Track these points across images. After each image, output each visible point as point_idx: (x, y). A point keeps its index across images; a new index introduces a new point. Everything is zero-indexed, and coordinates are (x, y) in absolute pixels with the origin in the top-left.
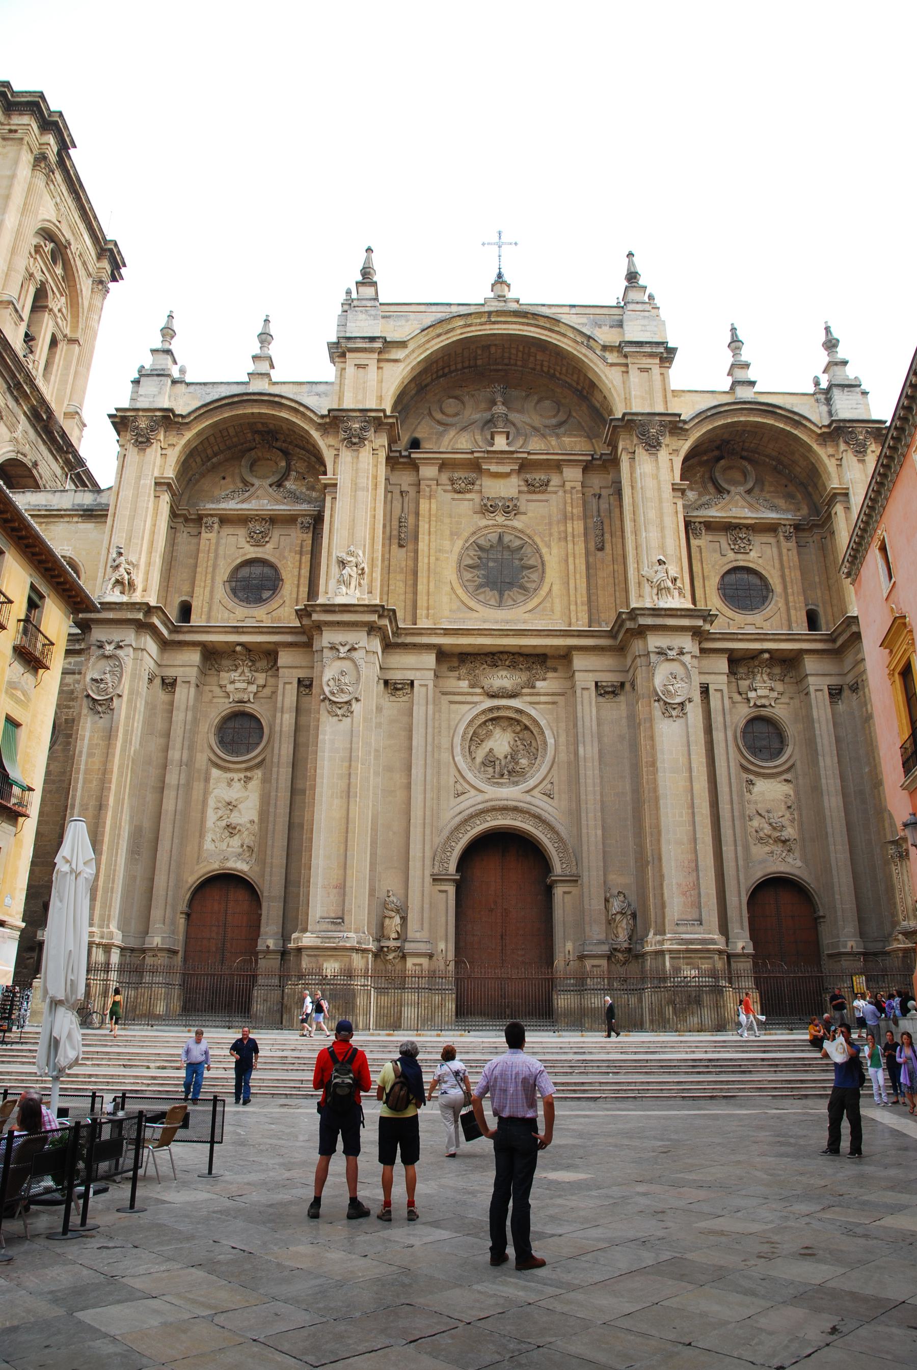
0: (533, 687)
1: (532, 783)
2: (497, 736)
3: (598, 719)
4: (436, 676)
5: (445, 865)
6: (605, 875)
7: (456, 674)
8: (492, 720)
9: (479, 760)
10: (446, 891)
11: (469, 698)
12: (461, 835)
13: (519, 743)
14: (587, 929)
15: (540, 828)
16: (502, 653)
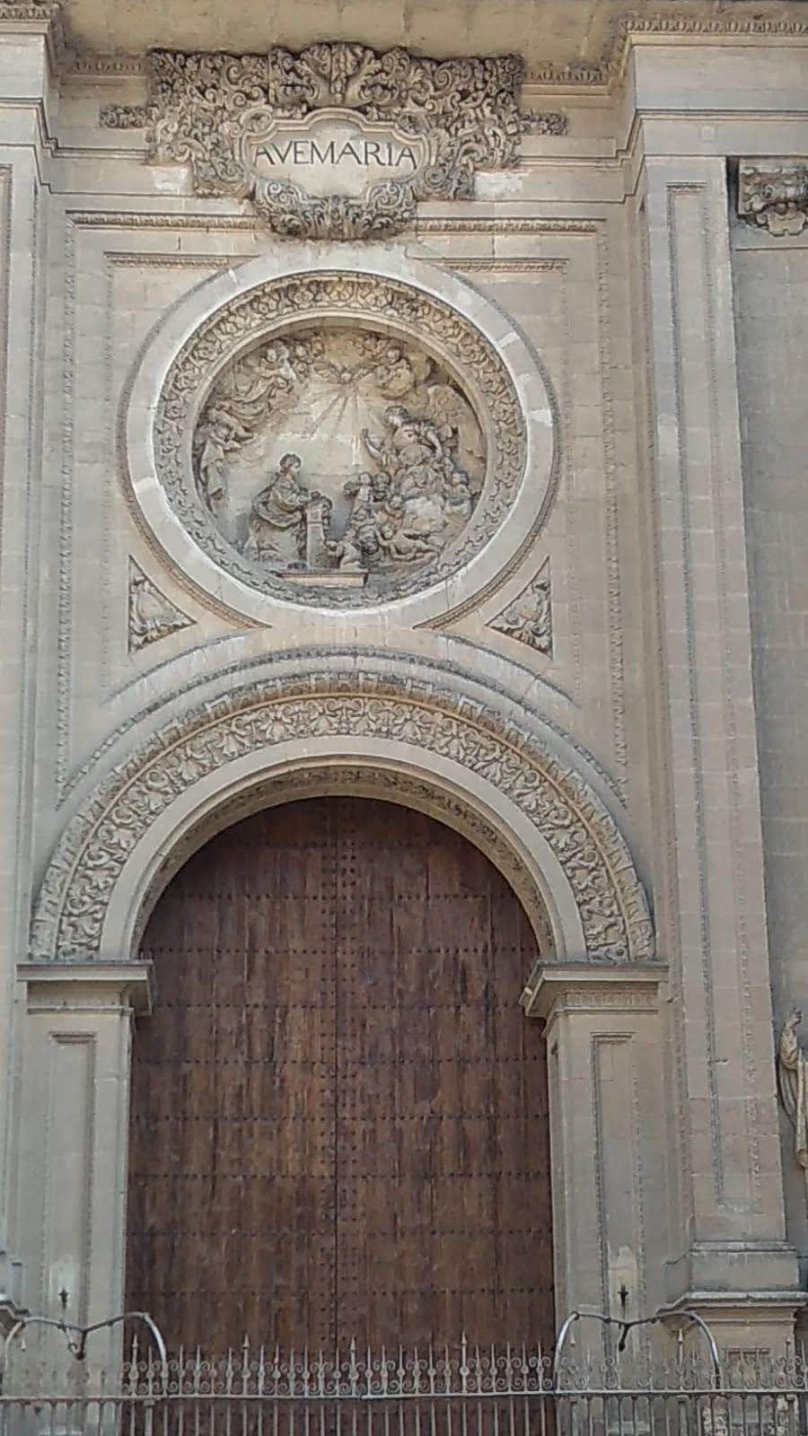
0: (466, 194)
1: (461, 585)
2: (316, 410)
3: (739, 317)
4: (53, 145)
5: (86, 925)
6: (774, 959)
7: (136, 137)
8: (291, 338)
9: (237, 504)
10: (87, 1039)
11: (193, 242)
12: (155, 801)
13: (405, 435)
14: (704, 1189)
15: (494, 768)
16: (329, 45)
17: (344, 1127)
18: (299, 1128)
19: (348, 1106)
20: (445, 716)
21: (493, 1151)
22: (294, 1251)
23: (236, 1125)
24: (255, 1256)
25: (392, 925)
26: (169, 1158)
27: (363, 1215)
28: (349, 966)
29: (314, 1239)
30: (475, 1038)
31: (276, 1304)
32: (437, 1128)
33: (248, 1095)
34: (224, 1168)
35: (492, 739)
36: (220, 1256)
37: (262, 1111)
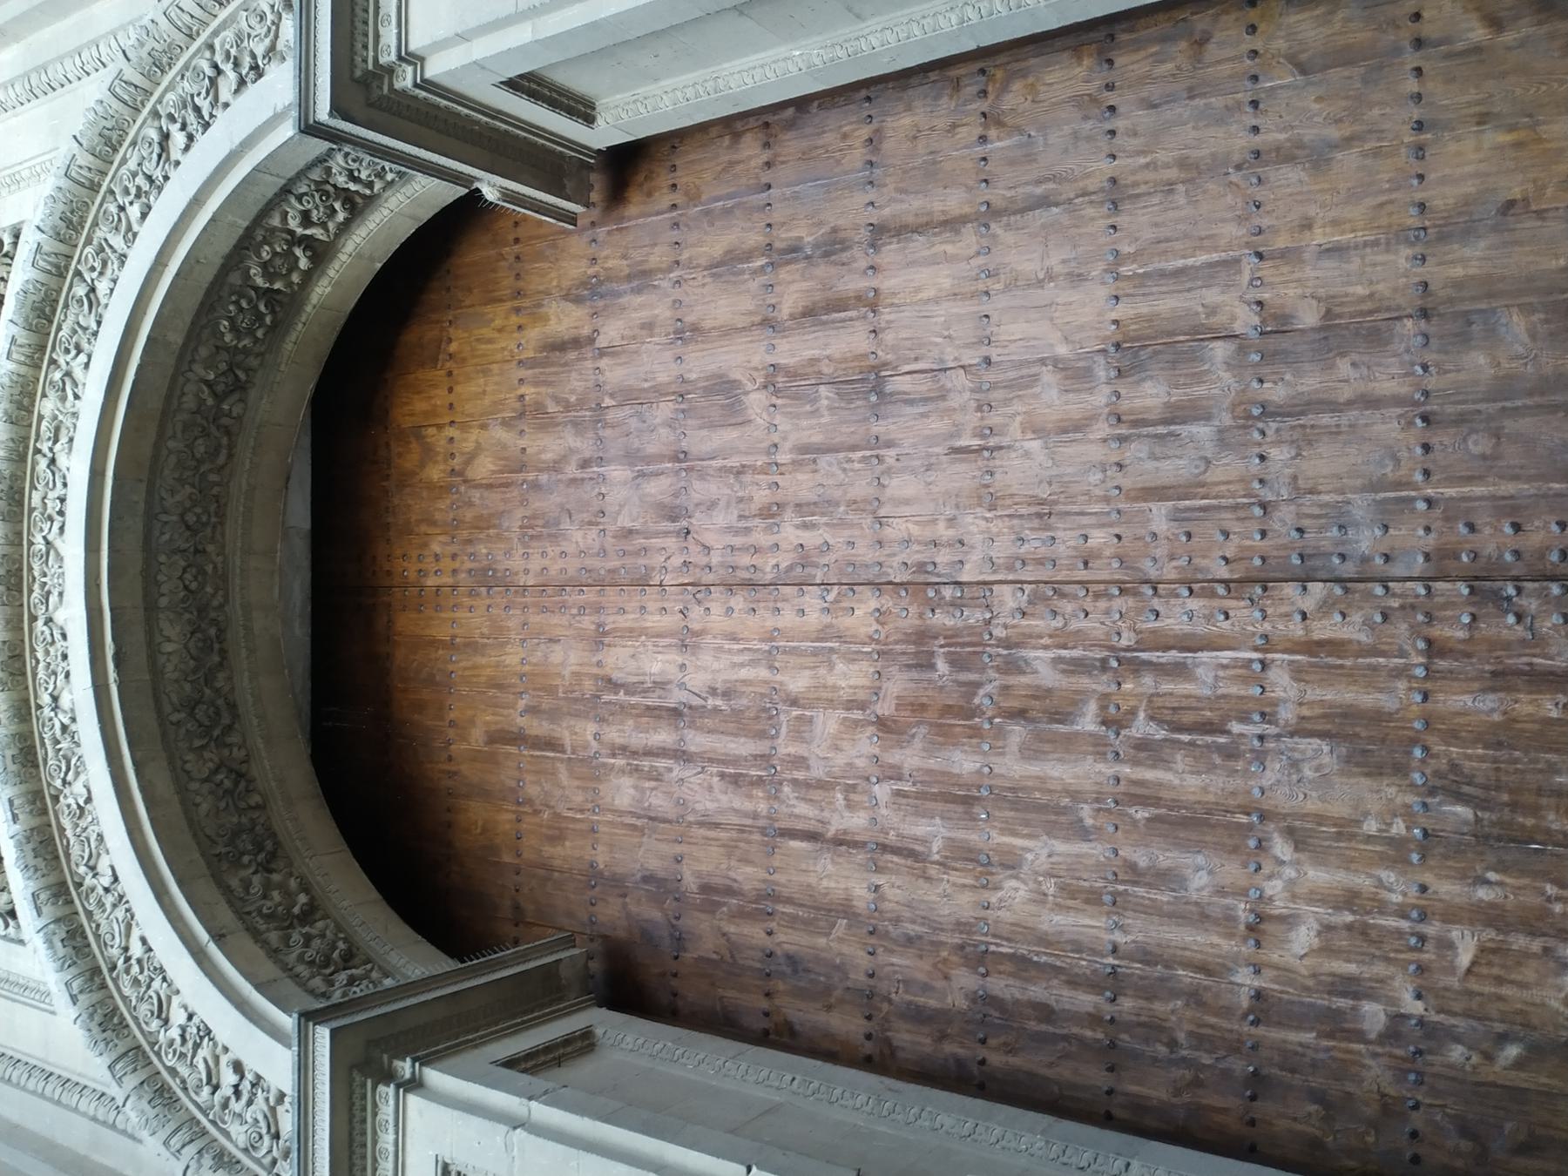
17: (790, 568)
18: (793, 660)
19: (757, 560)
20: (44, 395)
21: (833, 247)
22: (1024, 679)
23: (786, 789)
24: (1034, 769)
25: (490, 486)
26: (840, 940)
27: (952, 521)
28: (546, 562)
29: (999, 632)
30: (644, 315)
31: (1142, 727)
32: (793, 374)
33: (735, 761)
34: (856, 822)
35: (66, 306)
36: (1040, 851)
37: (762, 735)
